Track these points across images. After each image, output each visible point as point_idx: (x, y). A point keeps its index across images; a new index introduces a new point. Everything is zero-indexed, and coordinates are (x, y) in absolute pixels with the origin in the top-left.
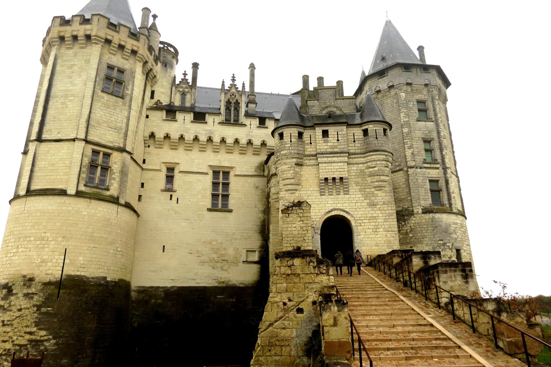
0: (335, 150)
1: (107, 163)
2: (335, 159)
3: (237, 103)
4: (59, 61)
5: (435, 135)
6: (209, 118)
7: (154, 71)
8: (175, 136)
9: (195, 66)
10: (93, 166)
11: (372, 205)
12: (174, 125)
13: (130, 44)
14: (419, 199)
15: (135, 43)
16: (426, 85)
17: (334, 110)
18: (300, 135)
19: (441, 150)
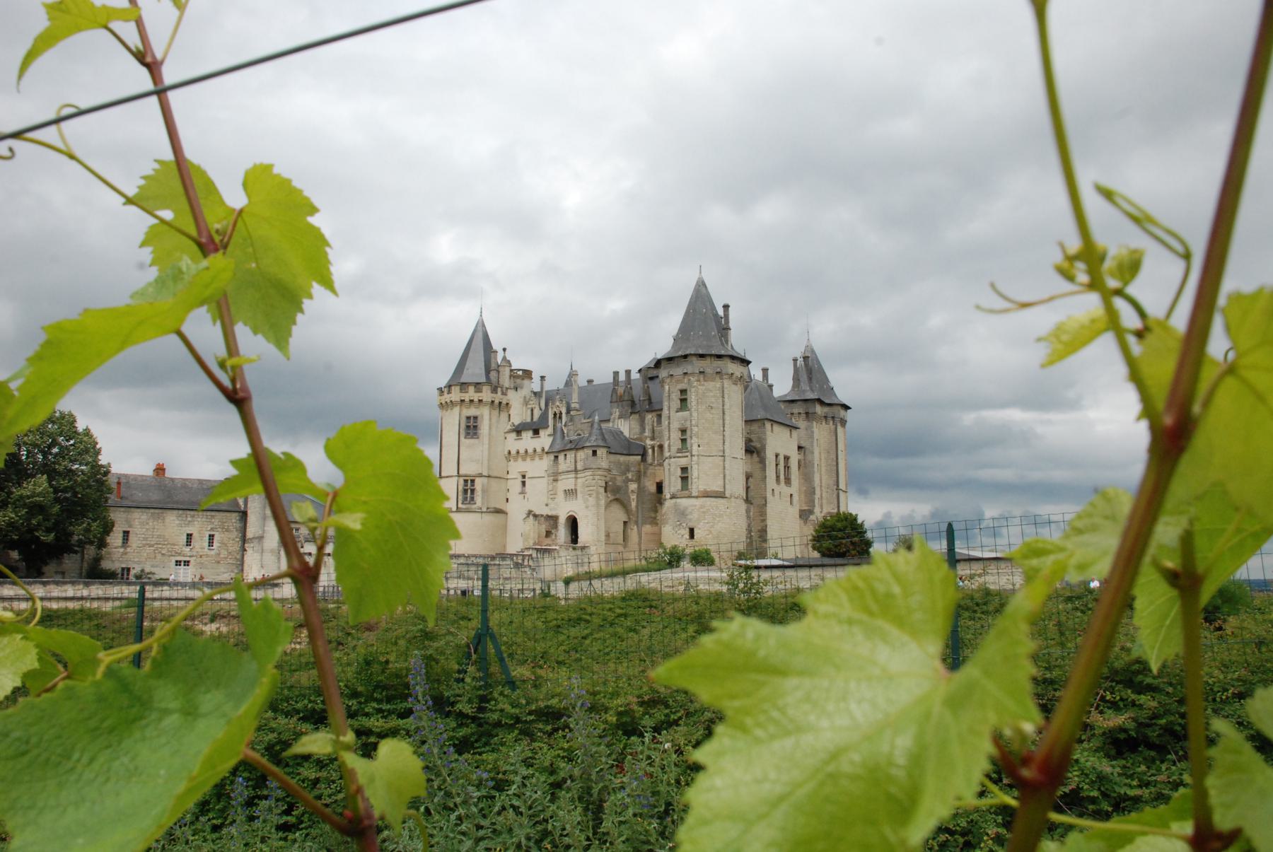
0: (569, 469)
1: (473, 485)
2: (569, 476)
3: (561, 413)
4: (444, 421)
5: (688, 423)
6: (542, 433)
7: (504, 402)
8: (522, 451)
9: (543, 378)
10: (465, 491)
11: (587, 507)
12: (521, 442)
13: (476, 397)
14: (669, 486)
15: (479, 394)
16: (686, 374)
17: (580, 432)
18: (556, 457)
19: (691, 437)
